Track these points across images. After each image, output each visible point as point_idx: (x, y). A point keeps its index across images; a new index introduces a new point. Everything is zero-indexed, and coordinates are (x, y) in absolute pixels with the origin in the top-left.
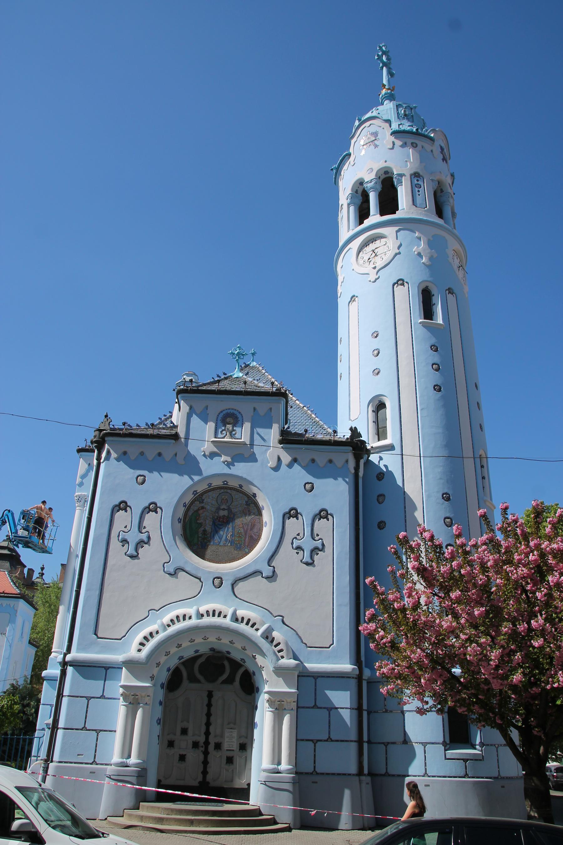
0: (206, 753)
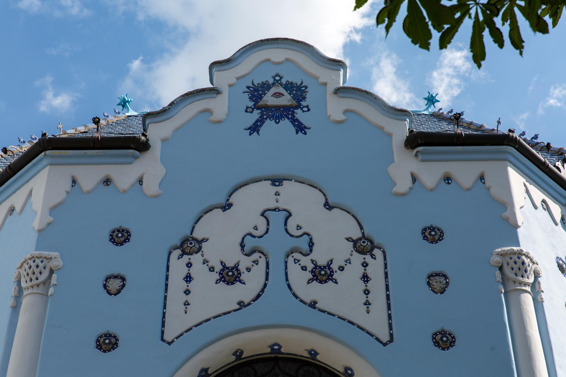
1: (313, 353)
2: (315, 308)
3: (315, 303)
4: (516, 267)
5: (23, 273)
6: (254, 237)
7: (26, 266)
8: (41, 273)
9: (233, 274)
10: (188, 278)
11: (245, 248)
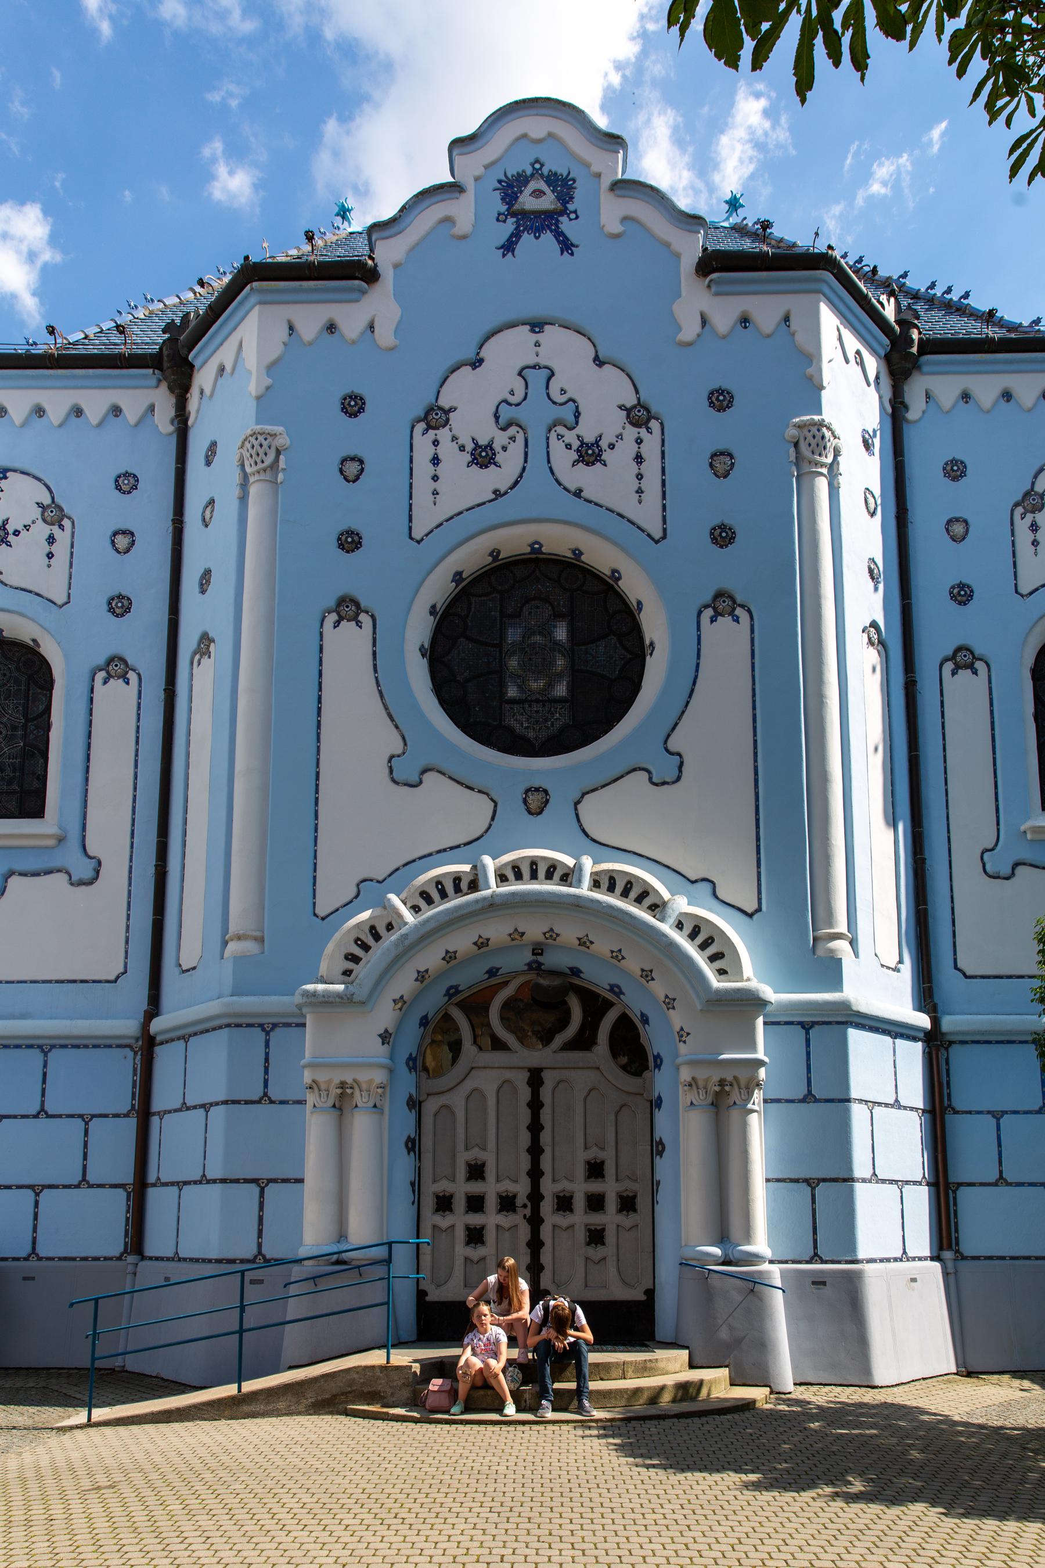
0: (535, 1221)
1: (577, 553)
2: (580, 497)
3: (581, 491)
4: (813, 442)
5: (246, 455)
6: (510, 404)
7: (248, 445)
8: (266, 454)
9: (487, 455)
10: (436, 460)
11: (500, 420)
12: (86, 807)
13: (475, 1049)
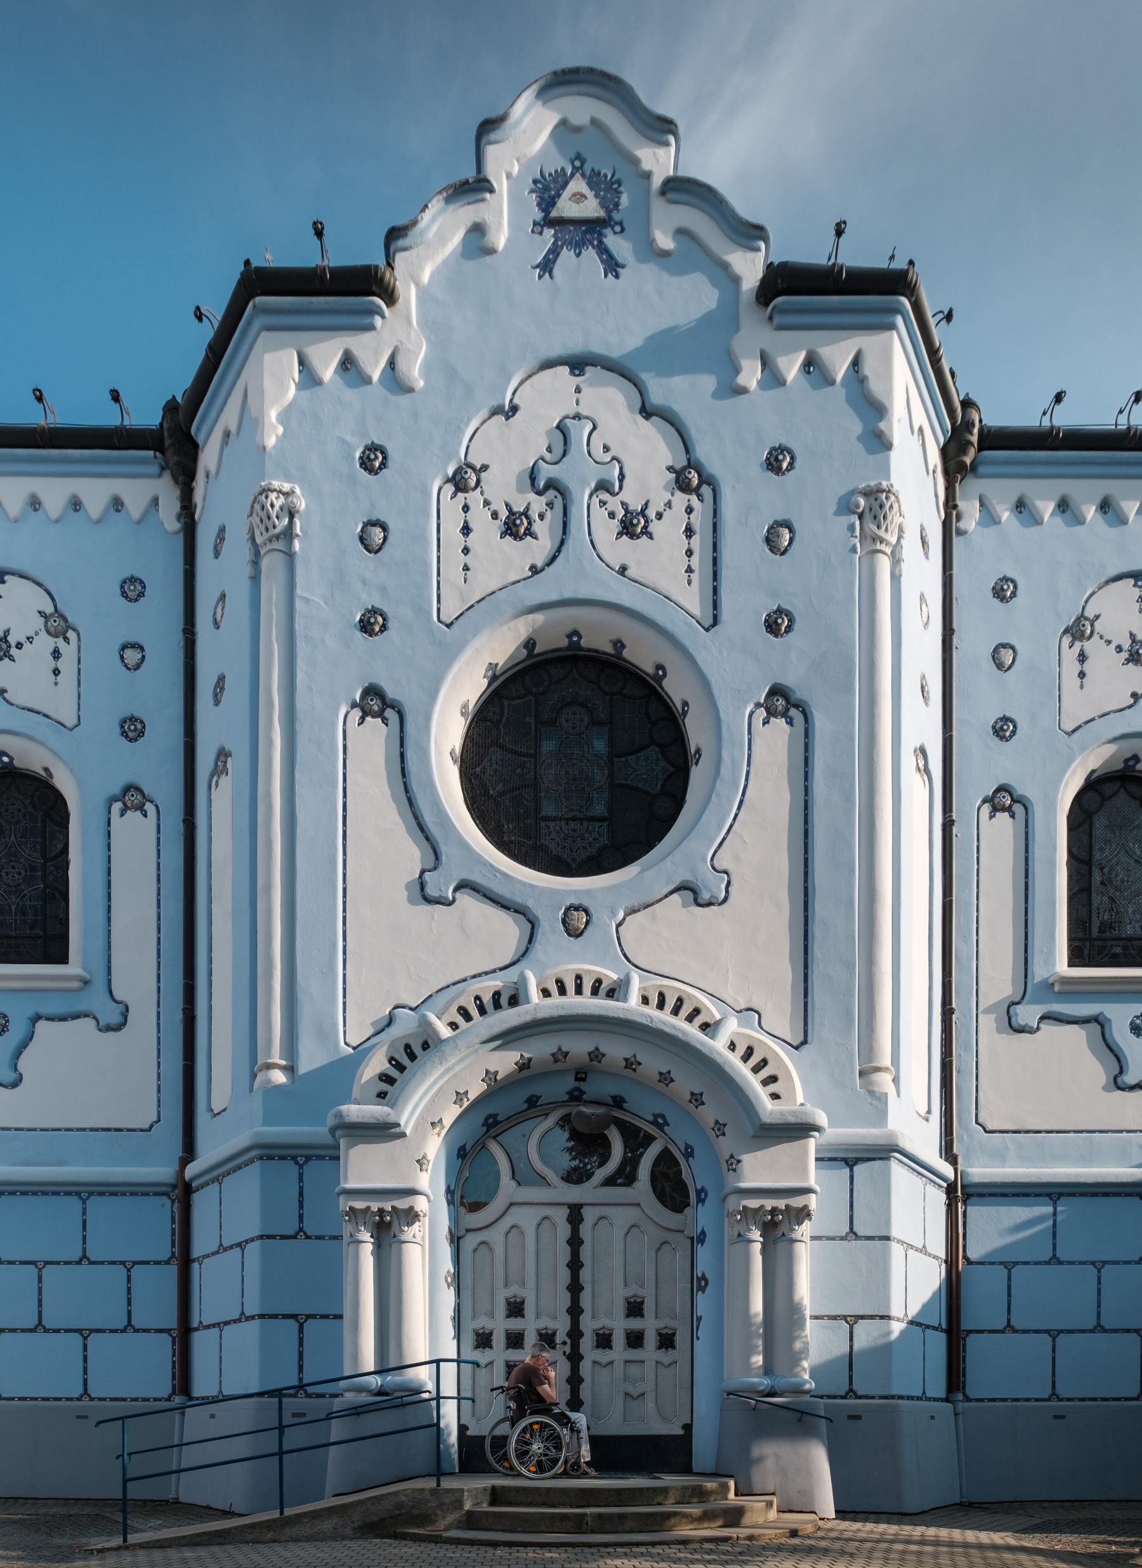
0: (575, 1358)
10: (466, 530)
12: (109, 949)
13: (513, 1184)
